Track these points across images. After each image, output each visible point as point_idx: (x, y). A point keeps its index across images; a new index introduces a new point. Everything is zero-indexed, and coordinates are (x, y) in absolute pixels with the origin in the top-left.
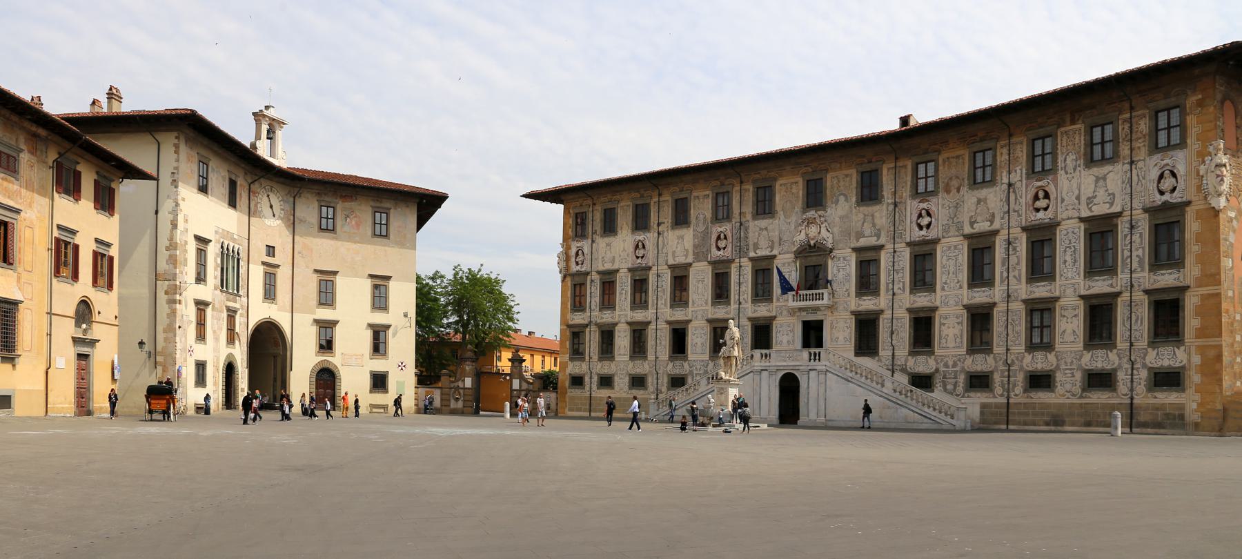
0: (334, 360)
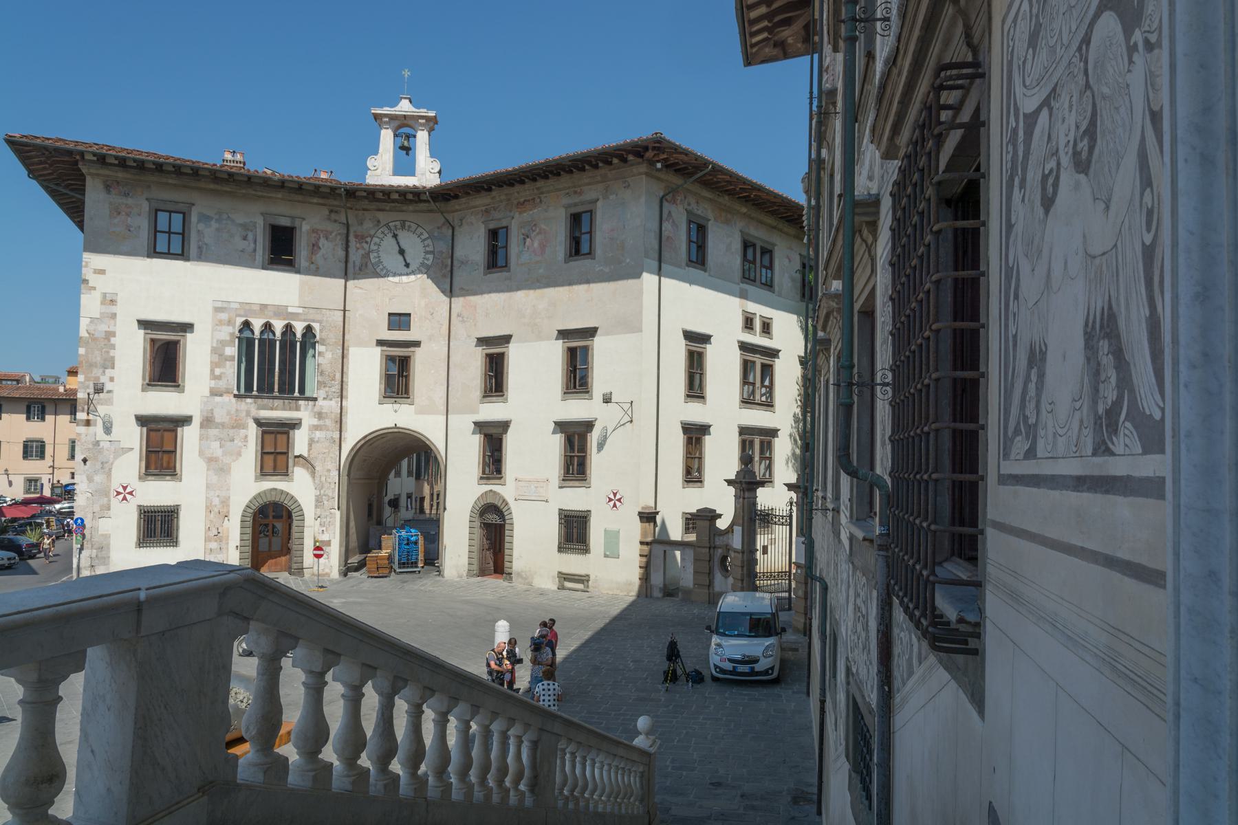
0: (507, 490)
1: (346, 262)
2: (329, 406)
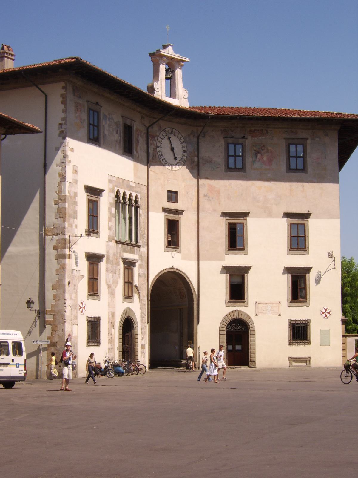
2: (143, 249)
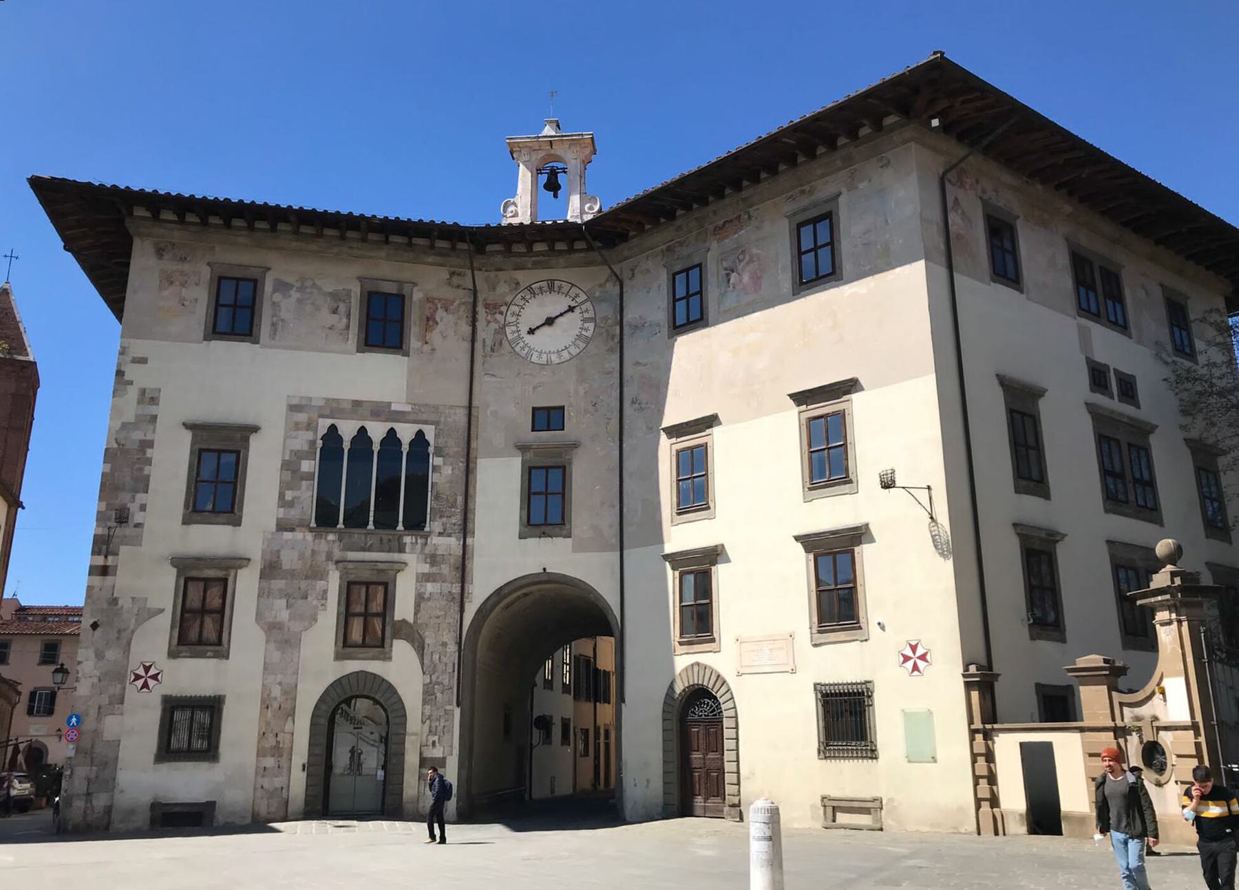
0: (722, 660)
1: (473, 341)
